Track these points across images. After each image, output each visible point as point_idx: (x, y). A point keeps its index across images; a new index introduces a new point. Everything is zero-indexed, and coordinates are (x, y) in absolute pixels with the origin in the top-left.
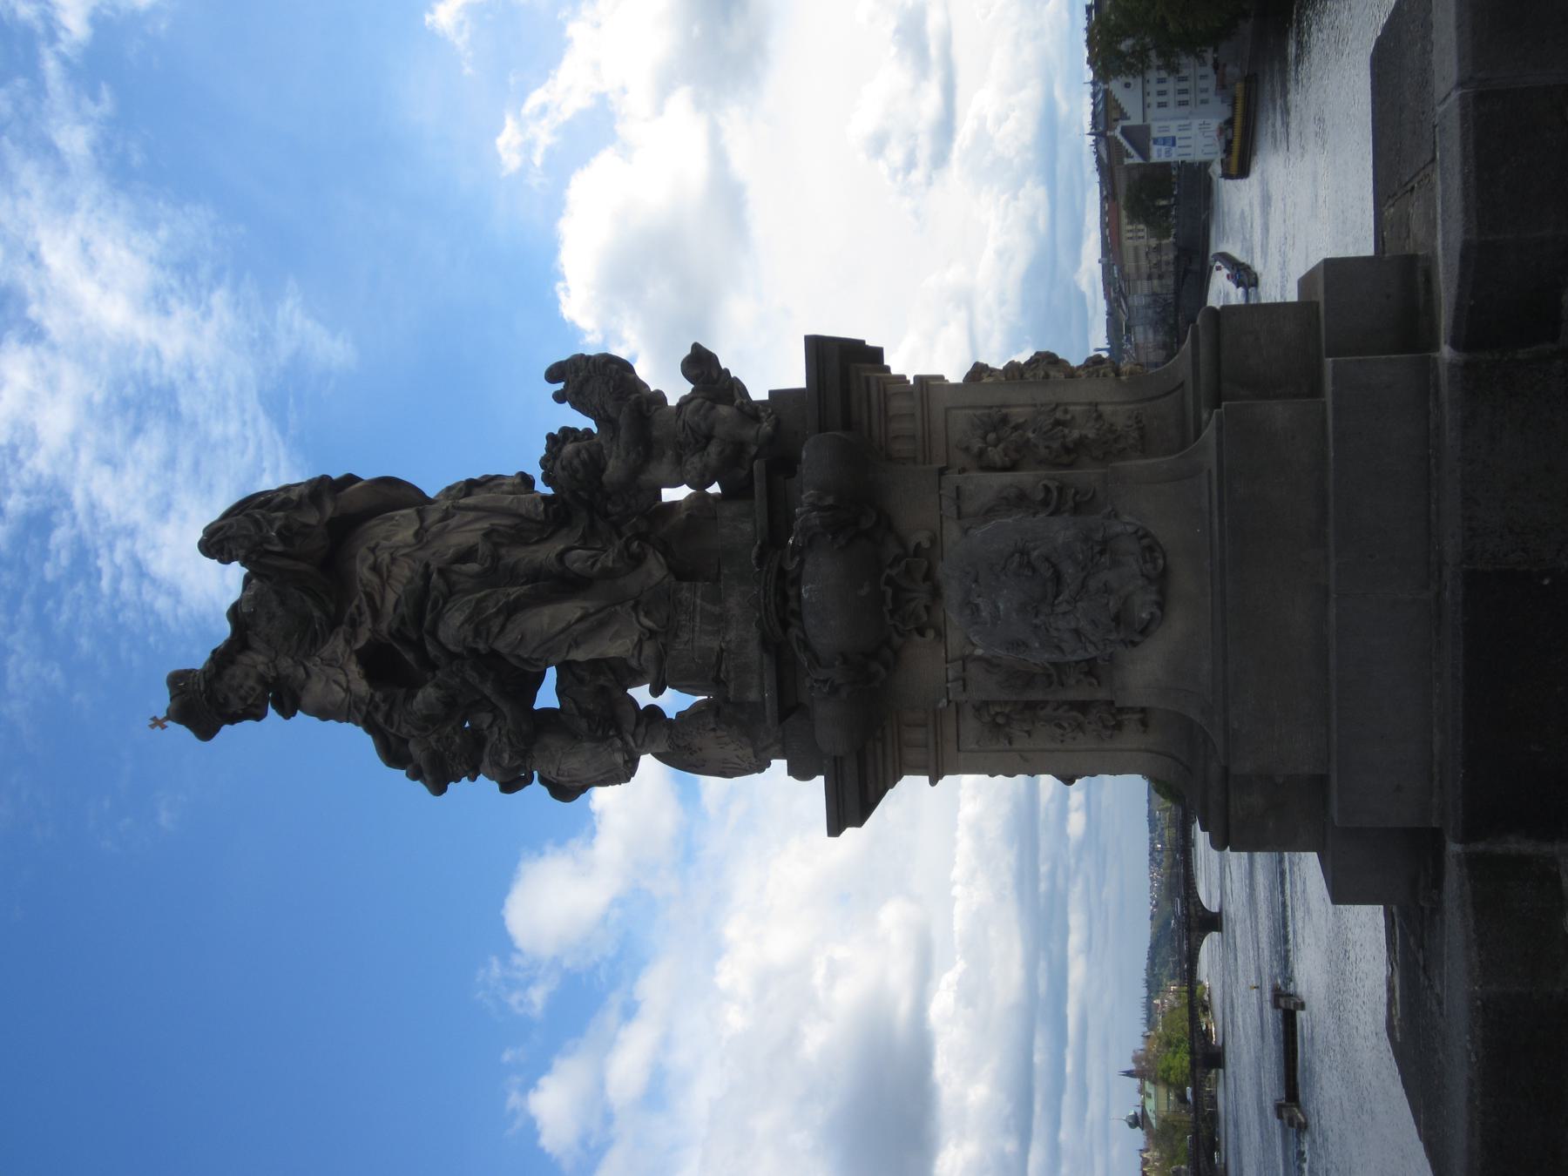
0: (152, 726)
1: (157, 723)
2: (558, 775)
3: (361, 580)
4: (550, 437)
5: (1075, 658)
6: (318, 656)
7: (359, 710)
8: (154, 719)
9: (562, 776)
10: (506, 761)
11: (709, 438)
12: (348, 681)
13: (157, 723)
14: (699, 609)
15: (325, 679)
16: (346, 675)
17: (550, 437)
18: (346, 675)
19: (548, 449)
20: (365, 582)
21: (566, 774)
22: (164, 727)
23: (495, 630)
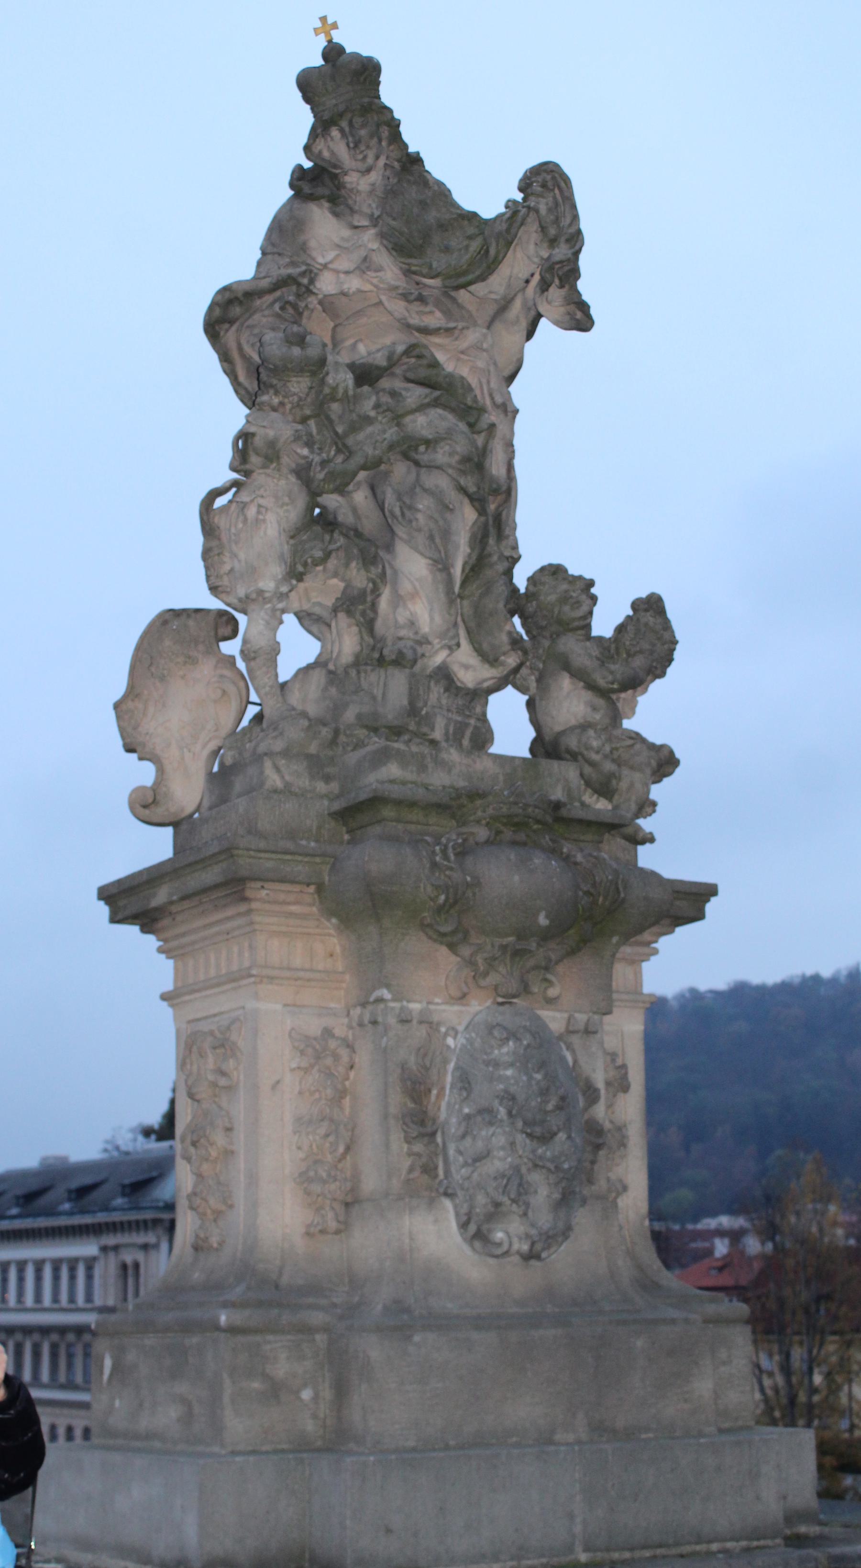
0: (323, 19)
1: (326, 26)
2: (259, 506)
3: (468, 328)
4: (591, 583)
5: (451, 1152)
6: (378, 248)
7: (303, 274)
8: (335, 26)
9: (259, 512)
10: (299, 451)
11: (618, 762)
12: (337, 272)
13: (326, 26)
14: (467, 721)
15: (346, 245)
16: (347, 273)
17: (591, 583)
18: (347, 273)
19: (580, 578)
20: (465, 332)
21: (261, 517)
22: (317, 31)
23: (462, 482)
